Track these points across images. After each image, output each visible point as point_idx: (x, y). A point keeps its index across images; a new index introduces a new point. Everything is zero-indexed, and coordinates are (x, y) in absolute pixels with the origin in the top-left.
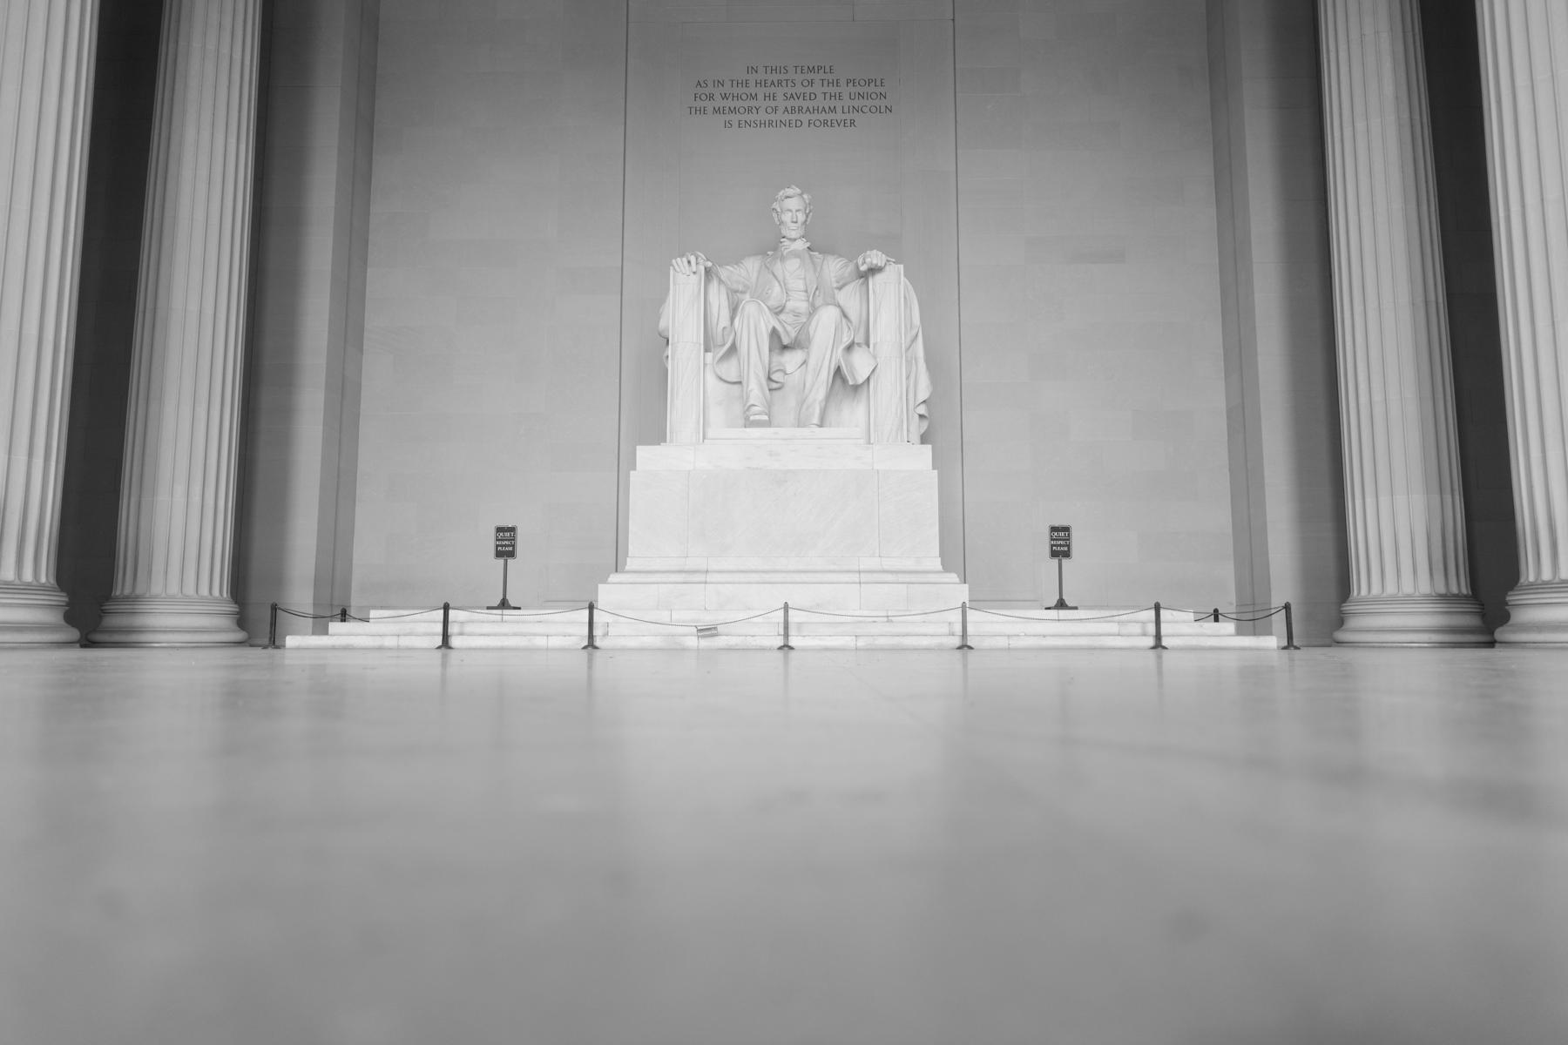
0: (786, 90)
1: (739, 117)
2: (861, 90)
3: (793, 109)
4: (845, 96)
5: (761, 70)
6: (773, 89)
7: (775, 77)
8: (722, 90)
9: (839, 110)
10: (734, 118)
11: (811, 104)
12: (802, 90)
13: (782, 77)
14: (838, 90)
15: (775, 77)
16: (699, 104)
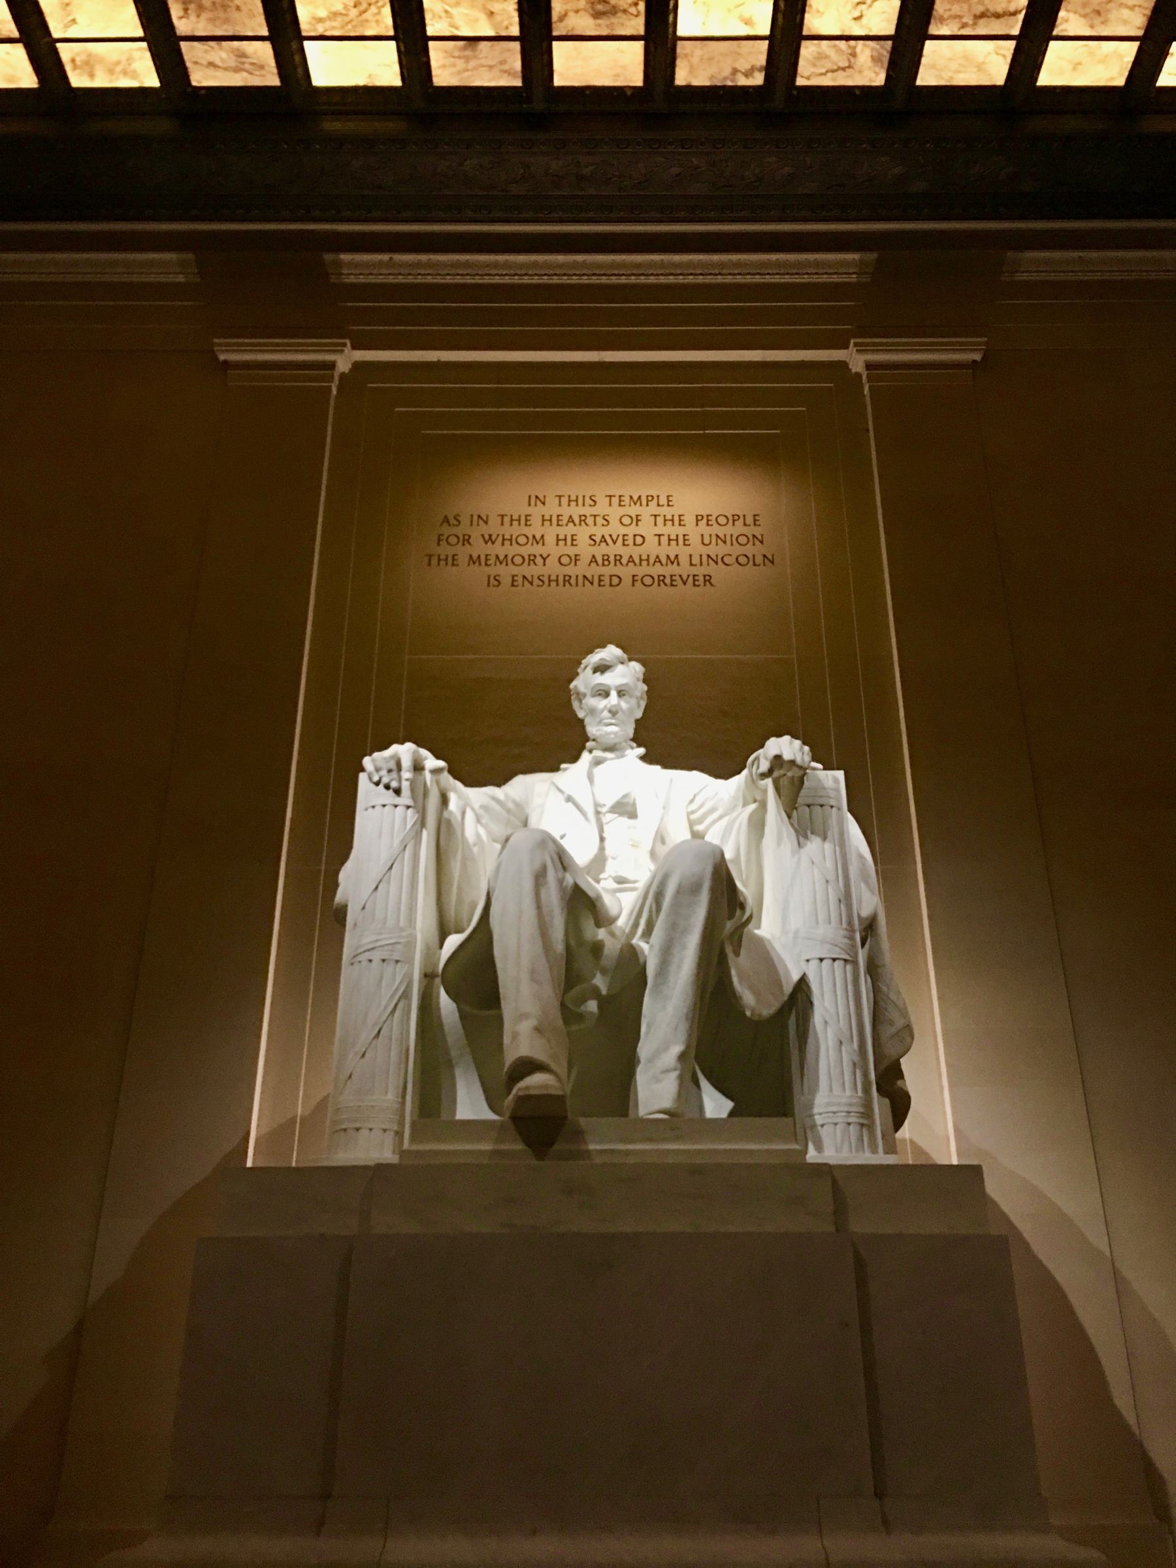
0: (592, 530)
1: (514, 570)
2: (722, 532)
3: (606, 559)
4: (695, 540)
5: (552, 501)
6: (570, 529)
7: (576, 511)
8: (484, 529)
9: (684, 560)
10: (505, 572)
11: (636, 552)
12: (623, 530)
13: (588, 511)
14: (681, 531)
15: (576, 511)
16: (445, 550)
